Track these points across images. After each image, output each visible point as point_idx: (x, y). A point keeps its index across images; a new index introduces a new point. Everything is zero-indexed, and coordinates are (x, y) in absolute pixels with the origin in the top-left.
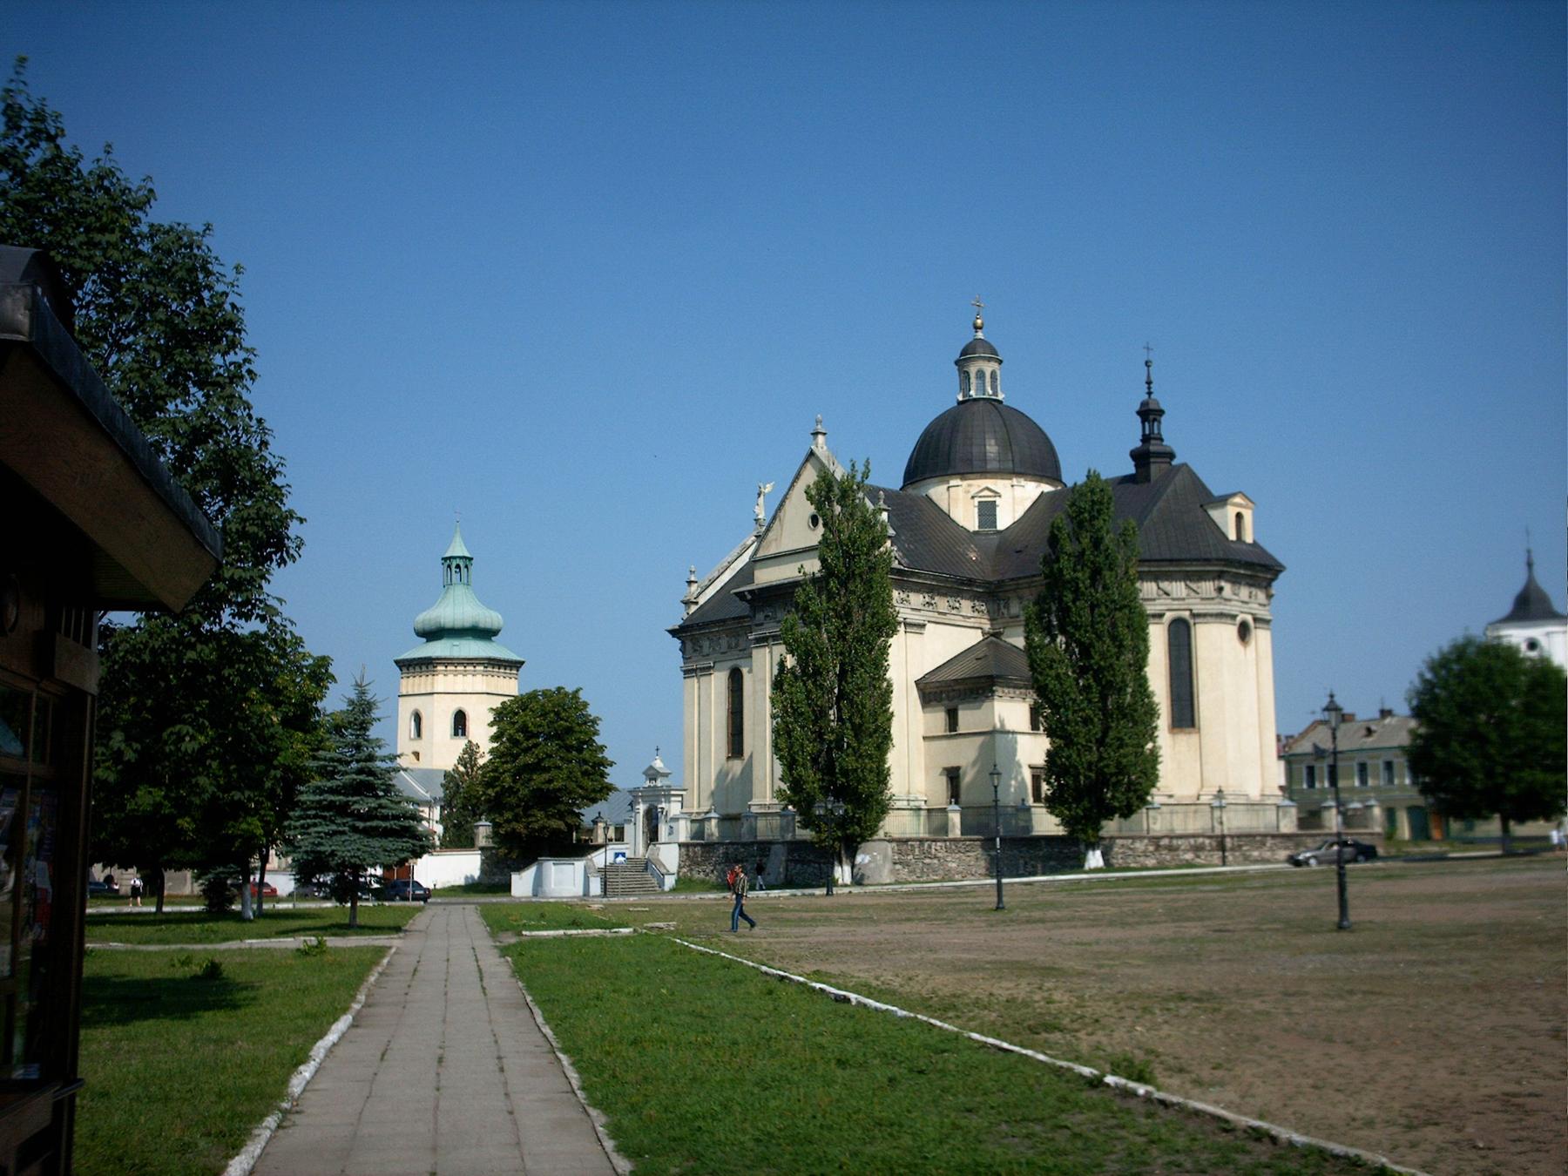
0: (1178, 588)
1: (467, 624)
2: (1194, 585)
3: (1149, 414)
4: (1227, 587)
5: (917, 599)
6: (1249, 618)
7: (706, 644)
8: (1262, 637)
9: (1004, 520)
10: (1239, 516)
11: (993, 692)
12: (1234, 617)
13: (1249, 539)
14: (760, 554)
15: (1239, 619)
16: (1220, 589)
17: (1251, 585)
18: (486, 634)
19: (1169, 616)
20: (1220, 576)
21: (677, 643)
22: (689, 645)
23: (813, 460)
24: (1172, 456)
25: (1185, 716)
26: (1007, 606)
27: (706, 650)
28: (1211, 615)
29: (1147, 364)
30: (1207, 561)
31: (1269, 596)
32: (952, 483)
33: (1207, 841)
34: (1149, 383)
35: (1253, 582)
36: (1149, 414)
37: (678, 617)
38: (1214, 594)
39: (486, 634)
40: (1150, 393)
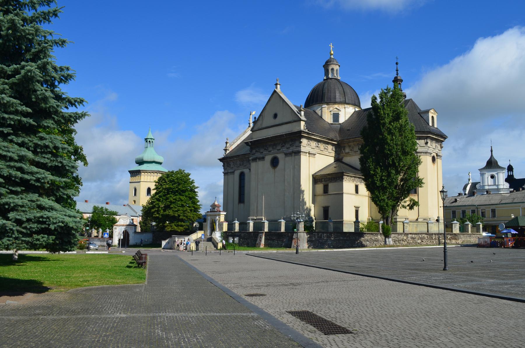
5: (313, 144)
7: (232, 164)
8: (439, 161)
9: (342, 119)
10: (433, 117)
11: (343, 178)
13: (436, 126)
14: (255, 129)
15: (432, 155)
16: (427, 143)
18: (160, 163)
21: (222, 164)
22: (226, 164)
23: (275, 94)
24: (405, 96)
26: (344, 149)
27: (232, 166)
28: (423, 152)
31: (442, 147)
32: (323, 106)
33: (426, 236)
35: (437, 141)
37: (222, 155)
39: (160, 163)
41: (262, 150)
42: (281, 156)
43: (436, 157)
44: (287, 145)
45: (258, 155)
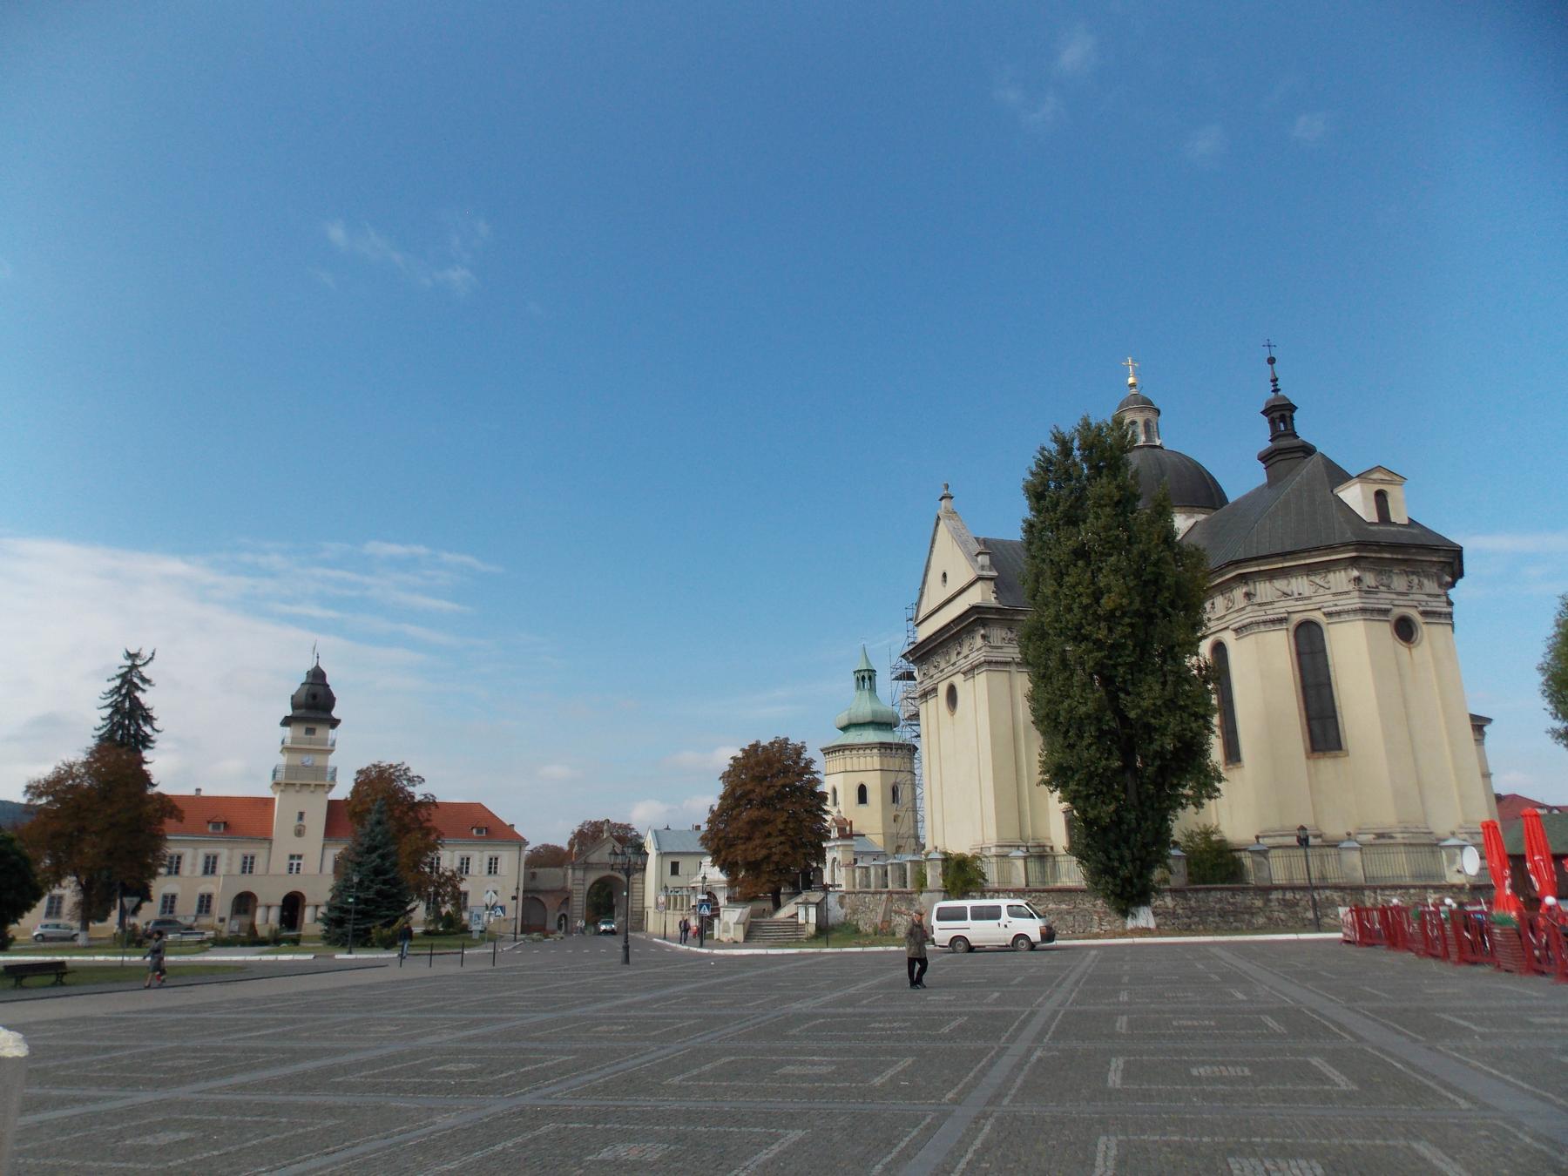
0: (1300, 584)
1: (869, 719)
2: (1318, 579)
3: (1280, 413)
4: (1370, 579)
6: (1414, 614)
12: (1386, 612)
14: (921, 617)
15: (1397, 612)
17: (1407, 573)
19: (1297, 618)
20: (1353, 562)
25: (1323, 729)
28: (1347, 612)
29: (1271, 361)
30: (1330, 548)
34: (1274, 380)
36: (1280, 413)
38: (1351, 587)
40: (1276, 391)
41: (932, 671)
42: (958, 680)
43: (1418, 619)
44: (965, 651)
45: (928, 684)
